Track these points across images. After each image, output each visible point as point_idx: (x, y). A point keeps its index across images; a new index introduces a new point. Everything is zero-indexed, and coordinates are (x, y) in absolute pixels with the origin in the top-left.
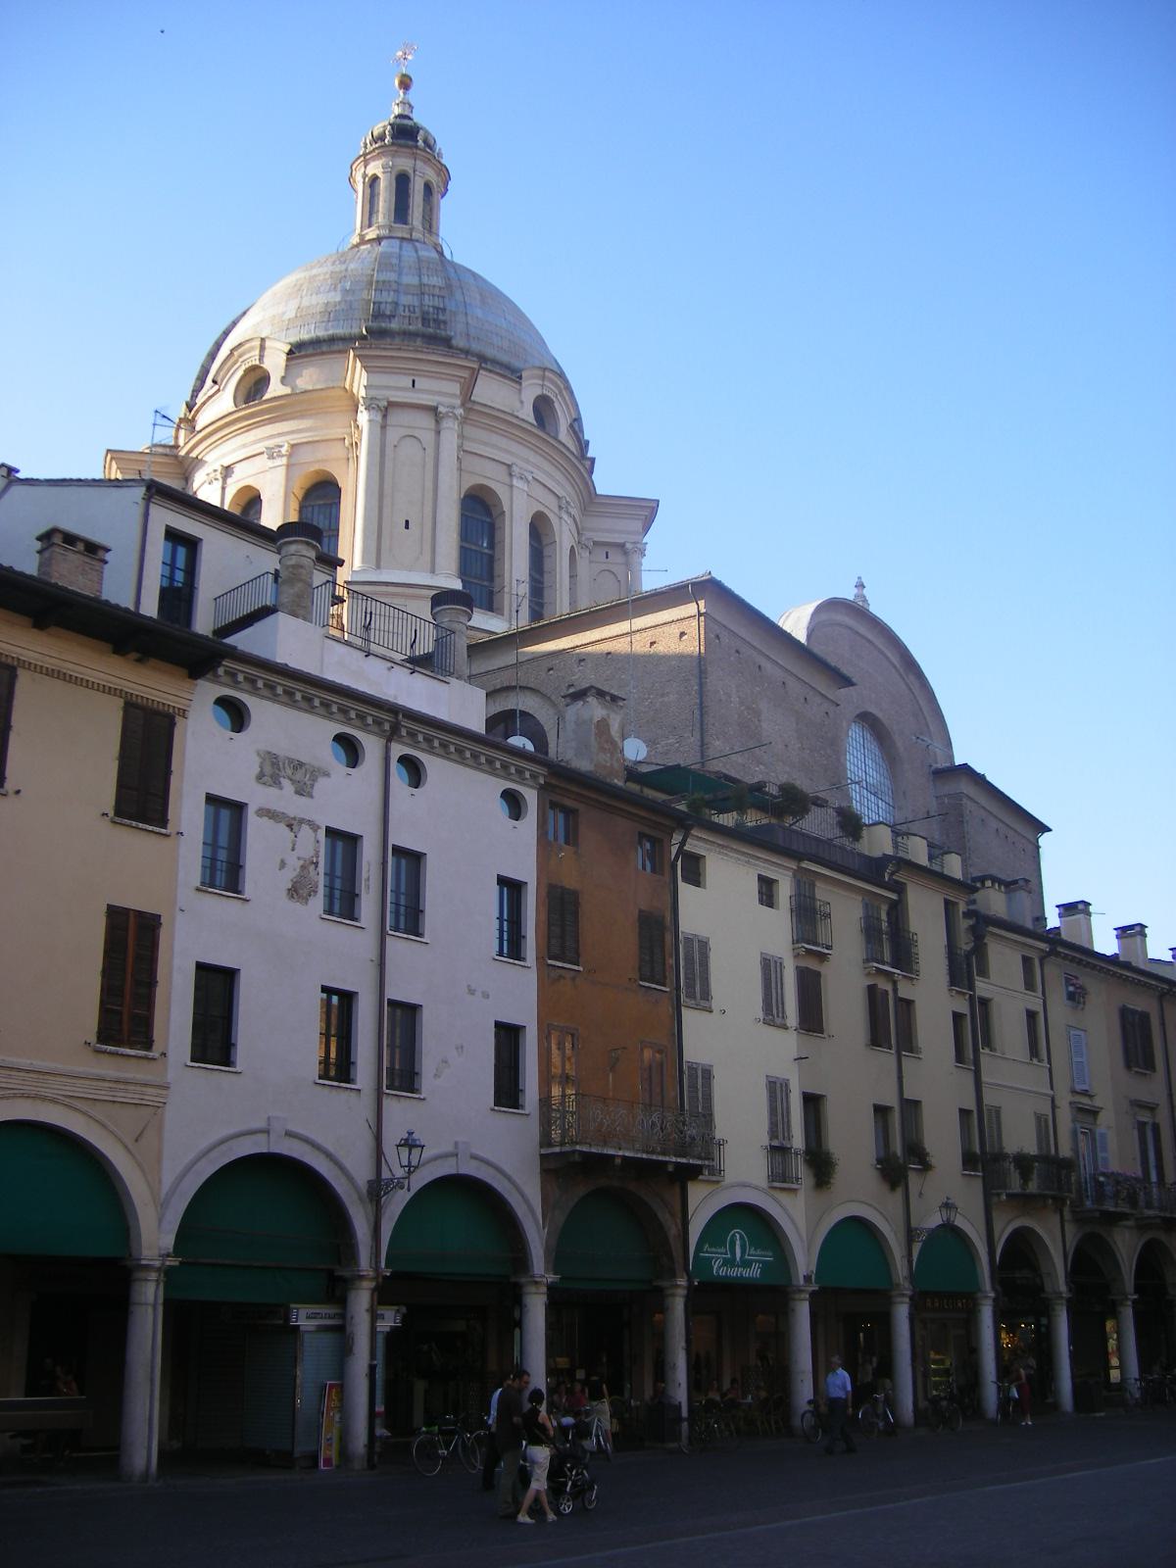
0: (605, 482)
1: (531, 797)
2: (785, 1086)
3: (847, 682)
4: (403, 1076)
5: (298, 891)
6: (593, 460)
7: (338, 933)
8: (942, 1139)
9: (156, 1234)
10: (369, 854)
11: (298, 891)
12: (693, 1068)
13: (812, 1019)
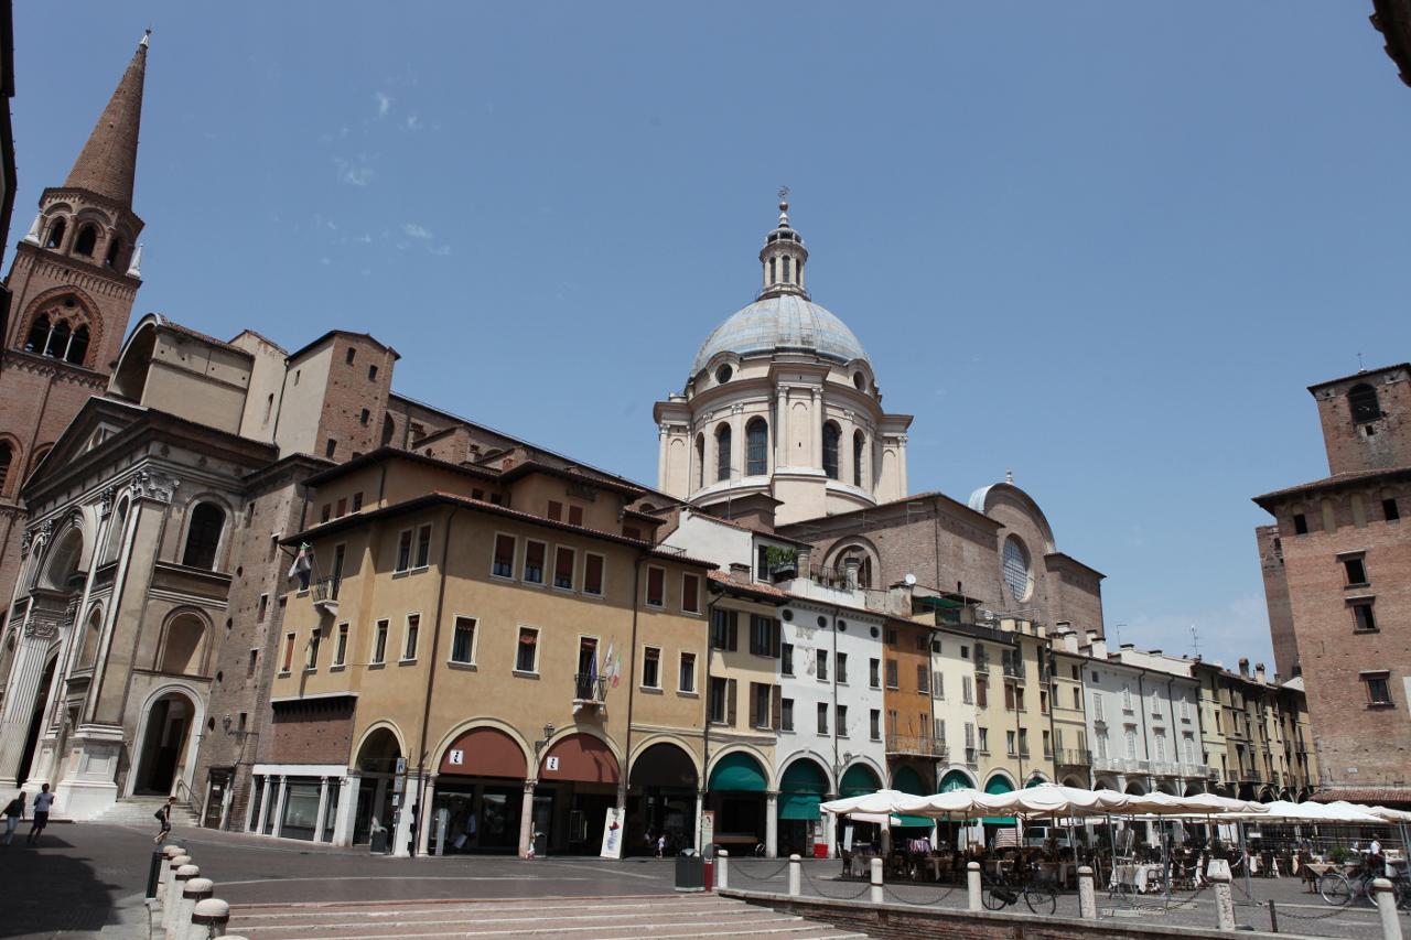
0: (887, 408)
2: (972, 725)
3: (1003, 526)
4: (841, 731)
5: (809, 672)
6: (881, 396)
7: (822, 686)
8: (1035, 743)
9: (774, 786)
11: (809, 672)
12: (938, 720)
13: (982, 703)
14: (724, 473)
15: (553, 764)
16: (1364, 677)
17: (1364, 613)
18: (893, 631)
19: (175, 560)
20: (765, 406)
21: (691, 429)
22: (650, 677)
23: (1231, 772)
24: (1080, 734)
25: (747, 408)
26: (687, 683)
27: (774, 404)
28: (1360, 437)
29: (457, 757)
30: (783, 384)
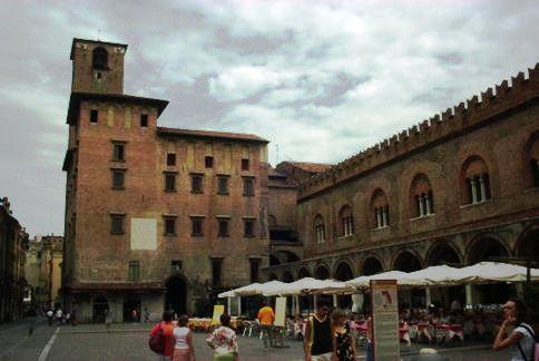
16: (112, 215)
17: (118, 175)
28: (93, 78)
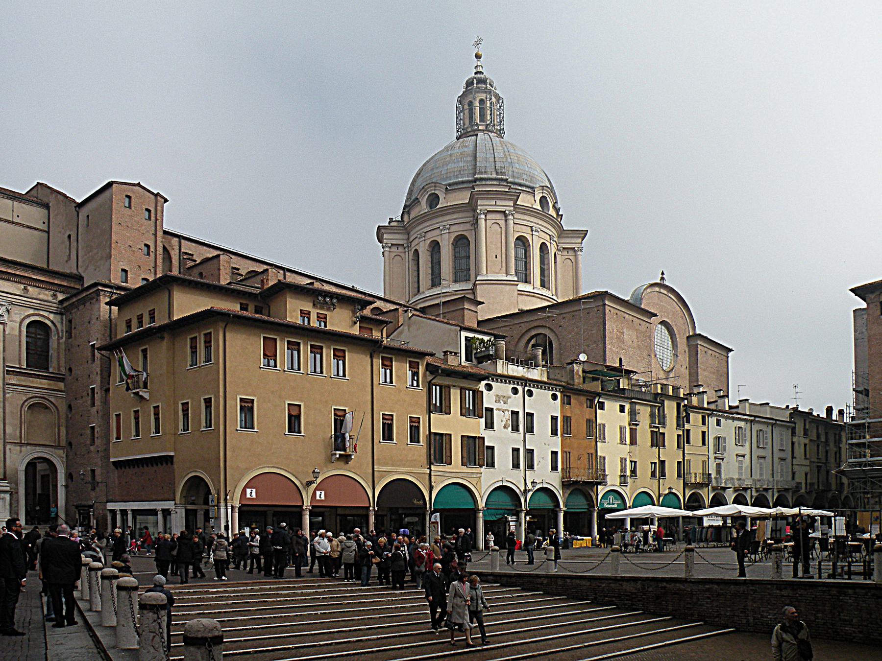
1: (559, 394)
7: (515, 435)
10: (521, 415)
11: (505, 427)
14: (436, 281)
15: (320, 495)
18: (568, 392)
19: (20, 364)
20: (468, 226)
21: (408, 247)
22: (388, 434)
23: (812, 484)
24: (704, 462)
25: (453, 228)
26: (415, 438)
27: (475, 223)
29: (251, 493)
30: (483, 205)
